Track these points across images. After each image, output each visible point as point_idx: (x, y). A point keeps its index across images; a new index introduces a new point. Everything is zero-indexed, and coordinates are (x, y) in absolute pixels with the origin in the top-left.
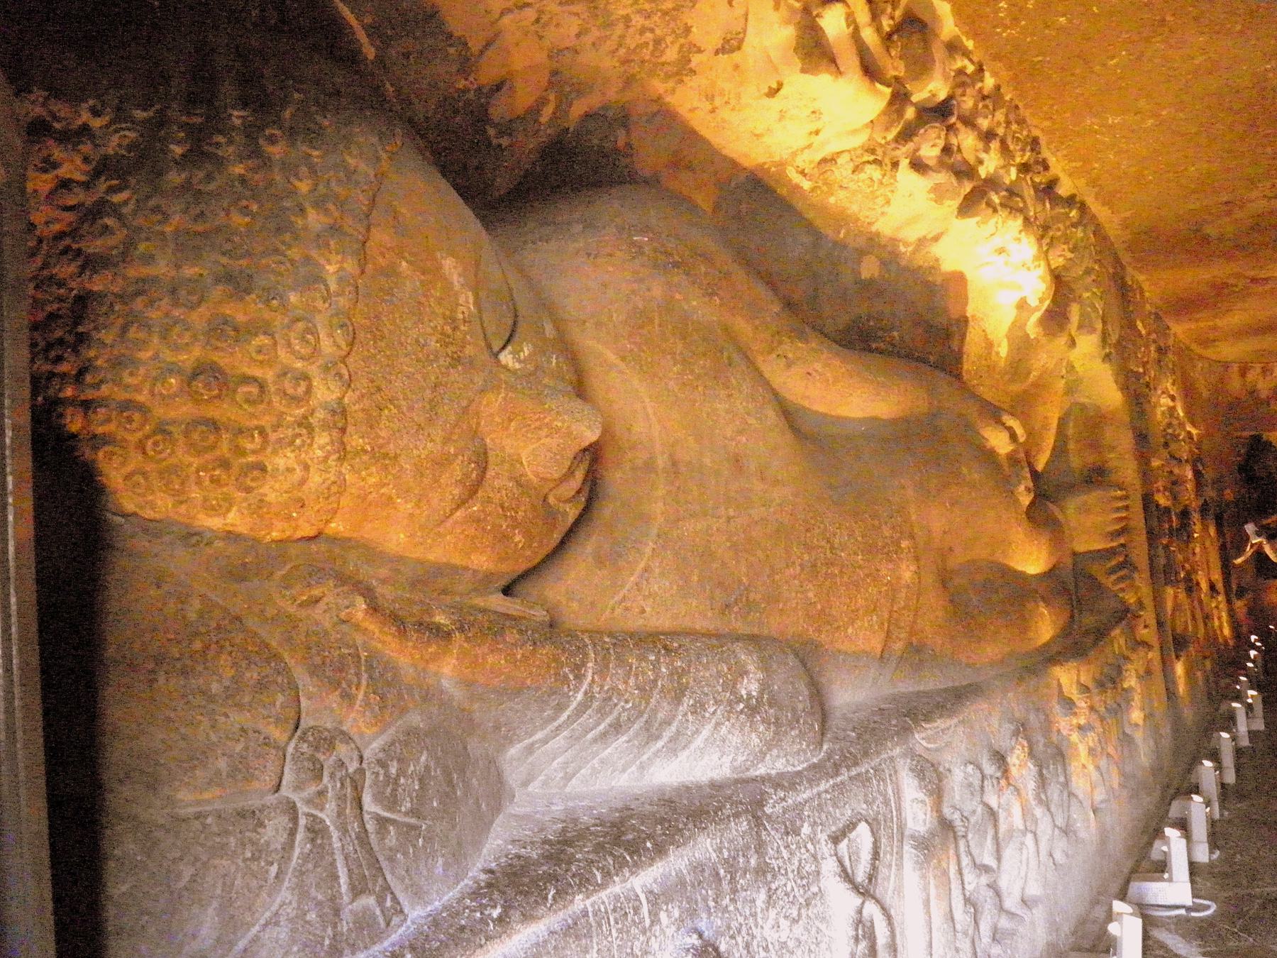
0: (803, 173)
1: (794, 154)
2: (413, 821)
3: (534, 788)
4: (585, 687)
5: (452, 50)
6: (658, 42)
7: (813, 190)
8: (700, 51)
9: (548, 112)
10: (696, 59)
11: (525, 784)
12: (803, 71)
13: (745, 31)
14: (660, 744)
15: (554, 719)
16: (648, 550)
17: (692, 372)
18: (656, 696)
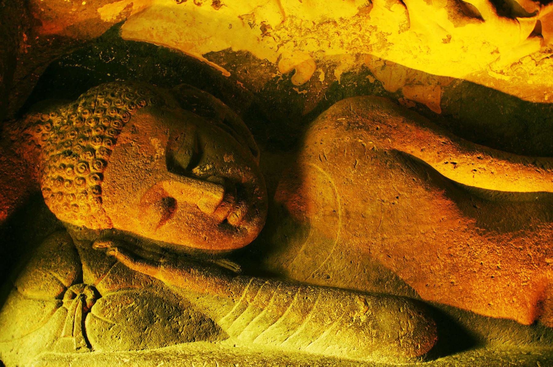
0: (502, 72)
1: (490, 66)
2: (110, 321)
3: (240, 337)
4: (242, 298)
5: (263, 65)
6: (363, 37)
7: (512, 80)
8: (388, 34)
9: (322, 78)
10: (390, 39)
11: (236, 335)
12: (456, 26)
13: (409, 19)
14: (297, 333)
15: (229, 310)
16: (332, 252)
17: (363, 173)
18: (289, 309)
